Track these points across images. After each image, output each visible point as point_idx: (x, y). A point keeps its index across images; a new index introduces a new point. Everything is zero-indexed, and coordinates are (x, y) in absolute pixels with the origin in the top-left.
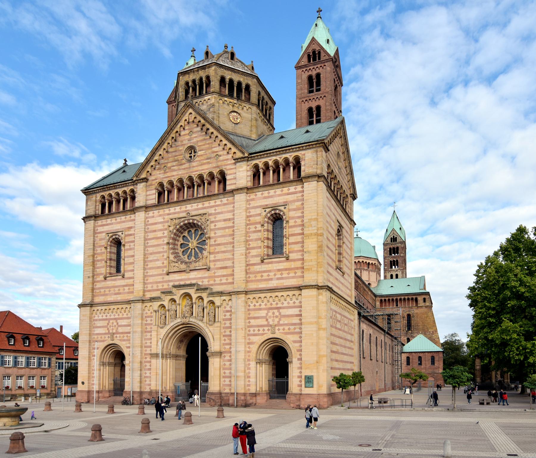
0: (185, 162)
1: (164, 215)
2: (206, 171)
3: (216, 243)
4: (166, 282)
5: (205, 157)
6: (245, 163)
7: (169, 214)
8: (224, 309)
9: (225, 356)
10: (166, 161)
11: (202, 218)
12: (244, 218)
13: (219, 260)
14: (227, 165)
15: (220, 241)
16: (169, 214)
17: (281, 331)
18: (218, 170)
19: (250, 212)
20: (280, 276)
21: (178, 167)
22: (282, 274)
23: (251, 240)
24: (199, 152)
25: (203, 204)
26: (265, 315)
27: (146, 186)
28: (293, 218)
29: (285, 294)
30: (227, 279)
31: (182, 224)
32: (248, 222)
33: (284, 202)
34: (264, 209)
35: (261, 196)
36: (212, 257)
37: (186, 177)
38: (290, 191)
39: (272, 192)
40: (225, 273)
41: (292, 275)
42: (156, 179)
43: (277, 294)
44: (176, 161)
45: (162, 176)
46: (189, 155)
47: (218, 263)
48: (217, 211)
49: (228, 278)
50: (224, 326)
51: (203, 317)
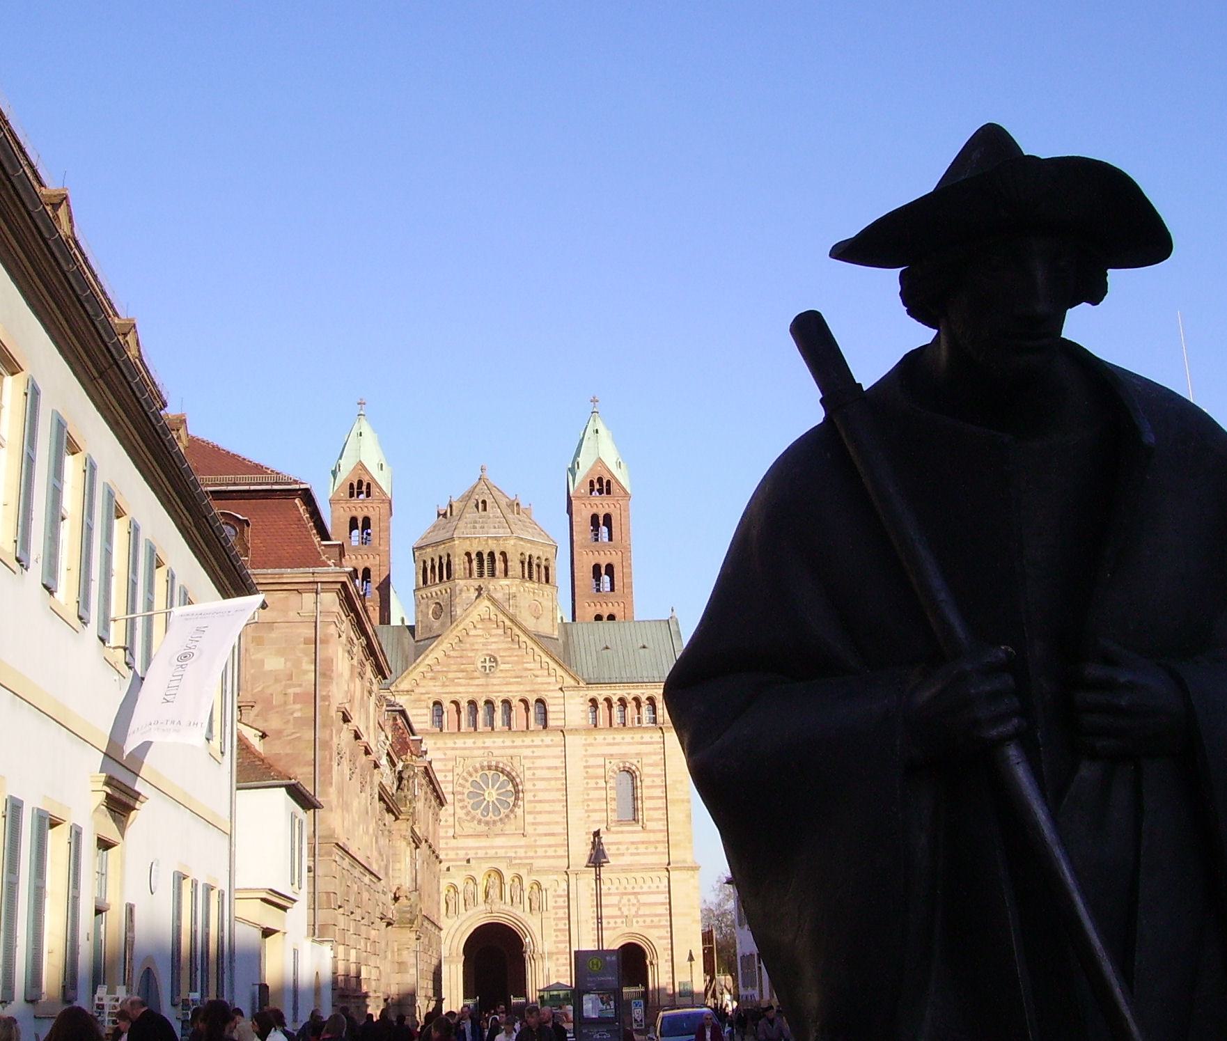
0: (479, 676)
1: (448, 748)
2: (516, 694)
3: (536, 798)
4: (453, 849)
6: (577, 693)
7: (453, 749)
8: (554, 893)
9: (557, 959)
10: (445, 669)
11: (513, 762)
12: (582, 767)
13: (541, 824)
14: (549, 691)
15: (541, 796)
16: (453, 749)
17: (641, 923)
18: (536, 697)
19: (587, 761)
20: (635, 851)
21: (467, 681)
22: (637, 848)
23: (591, 800)
24: (502, 665)
25: (513, 742)
26: (617, 903)
28: (649, 776)
29: (646, 875)
30: (555, 851)
31: (478, 765)
32: (585, 775)
33: (637, 754)
36: (529, 818)
38: (644, 740)
39: (618, 737)
40: (553, 843)
41: (652, 849)
43: (633, 875)
45: (438, 689)
47: (541, 827)
48: (535, 755)
49: (557, 849)
50: (554, 916)
51: (520, 902)
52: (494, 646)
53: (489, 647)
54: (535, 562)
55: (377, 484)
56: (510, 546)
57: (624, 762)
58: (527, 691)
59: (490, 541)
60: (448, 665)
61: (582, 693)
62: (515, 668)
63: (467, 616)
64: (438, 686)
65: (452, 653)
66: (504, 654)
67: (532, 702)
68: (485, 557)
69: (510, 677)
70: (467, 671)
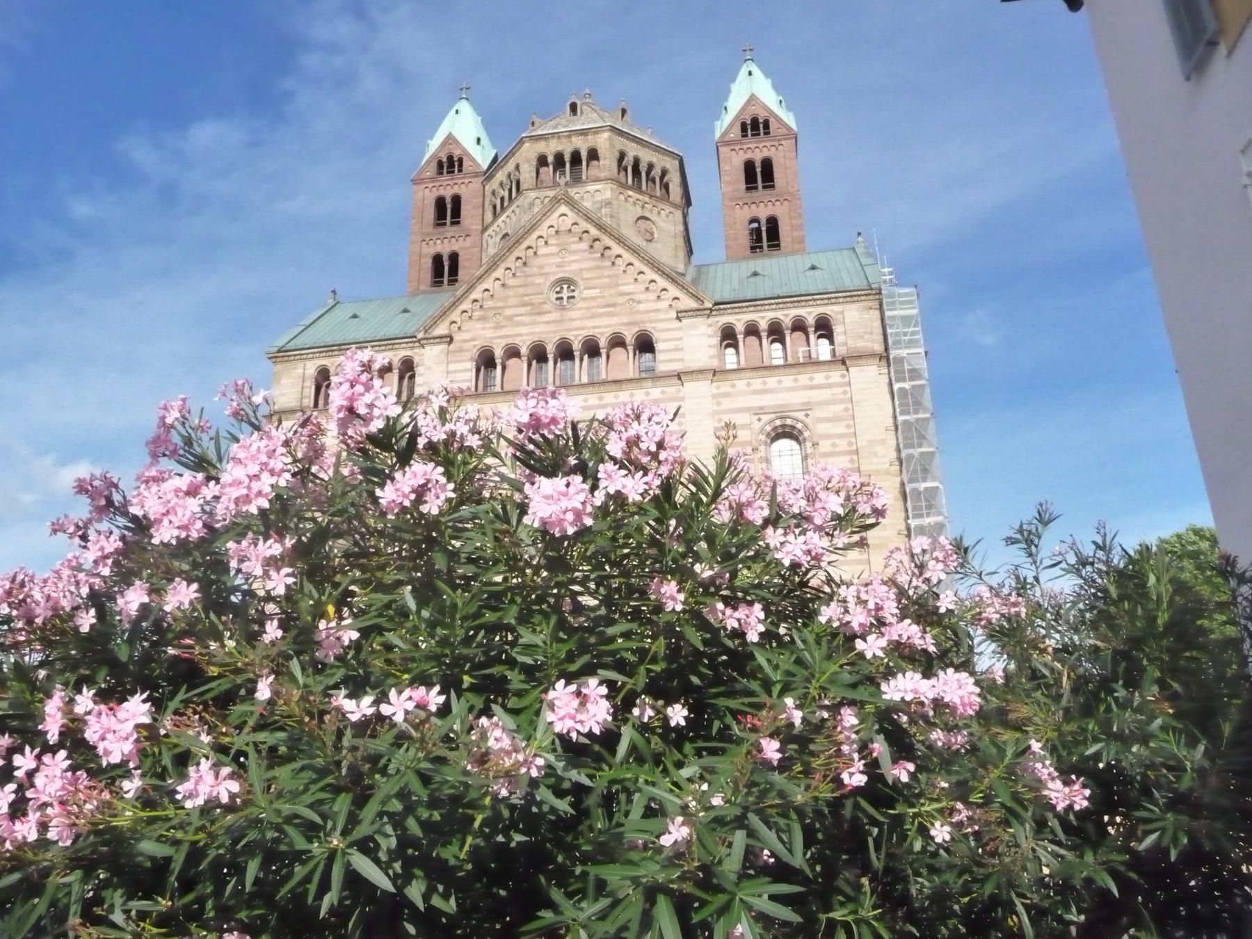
2: (605, 330)
5: (602, 301)
10: (500, 304)
18: (637, 329)
21: (533, 318)
24: (585, 292)
25: (601, 399)
27: (448, 352)
33: (803, 404)
34: (755, 414)
35: (746, 388)
37: (555, 340)
38: (815, 382)
39: (772, 381)
42: (472, 340)
44: (525, 305)
45: (488, 333)
46: (556, 296)
52: (574, 267)
53: (566, 269)
54: (643, 168)
55: (469, 156)
56: (602, 141)
57: (781, 418)
58: (623, 324)
59: (574, 139)
60: (505, 299)
61: (711, 320)
62: (606, 294)
63: (533, 227)
64: (490, 328)
65: (511, 282)
66: (589, 276)
67: (630, 338)
68: (567, 158)
69: (599, 307)
70: (532, 305)
